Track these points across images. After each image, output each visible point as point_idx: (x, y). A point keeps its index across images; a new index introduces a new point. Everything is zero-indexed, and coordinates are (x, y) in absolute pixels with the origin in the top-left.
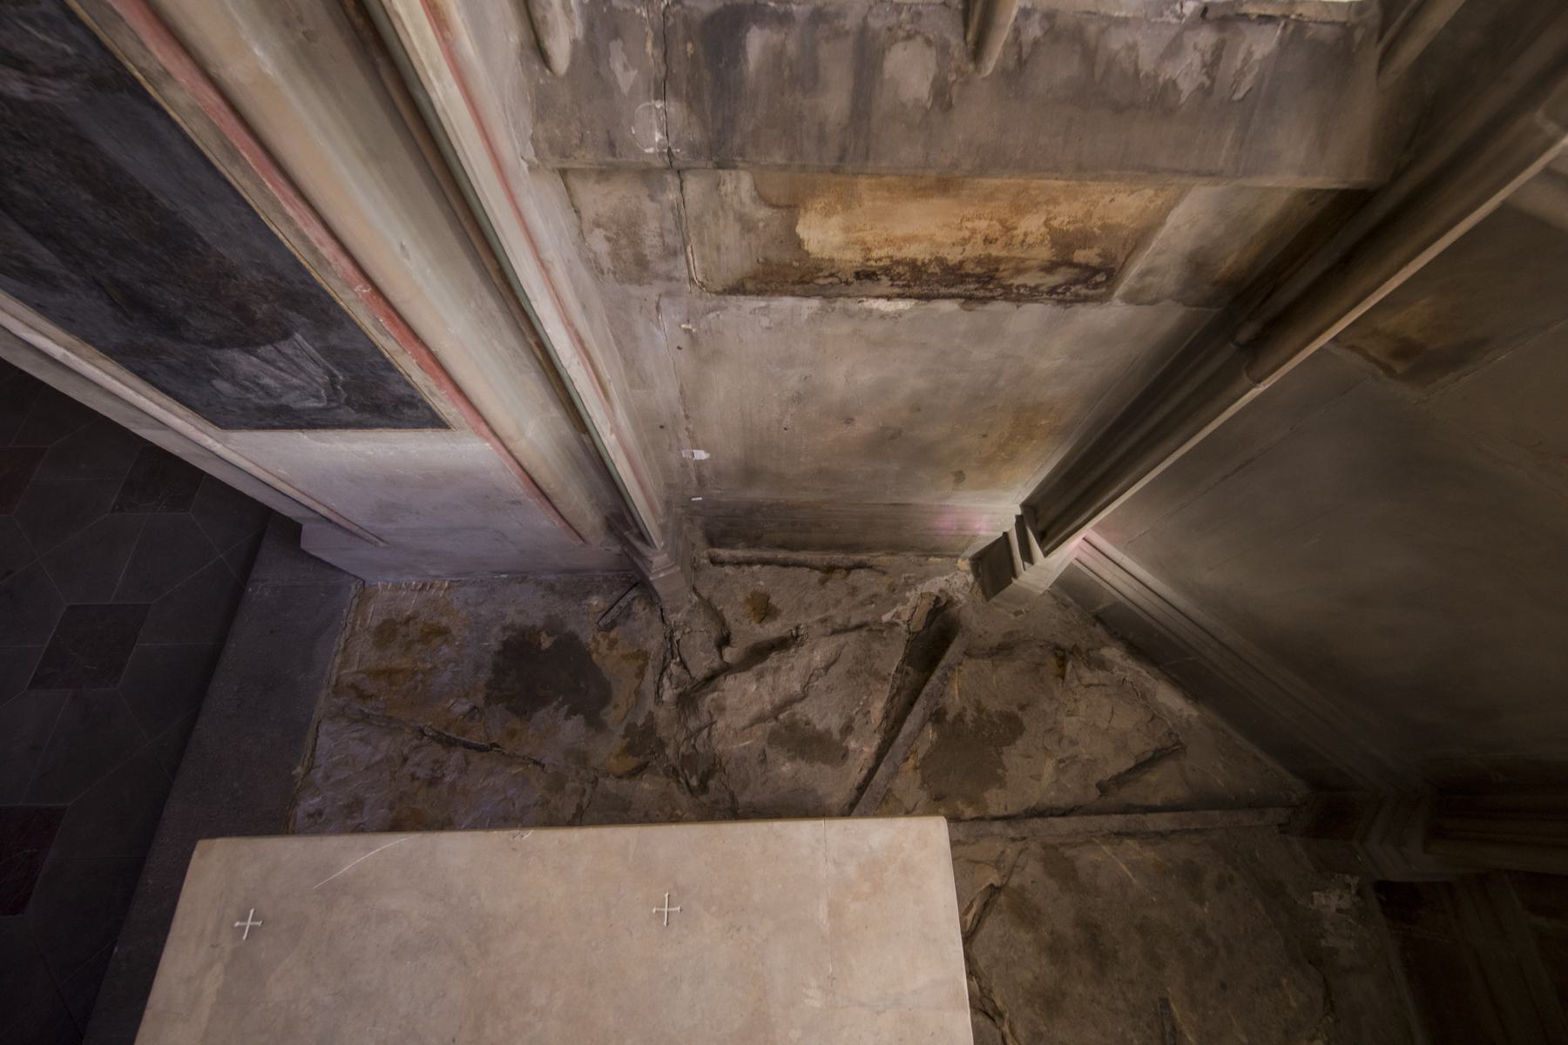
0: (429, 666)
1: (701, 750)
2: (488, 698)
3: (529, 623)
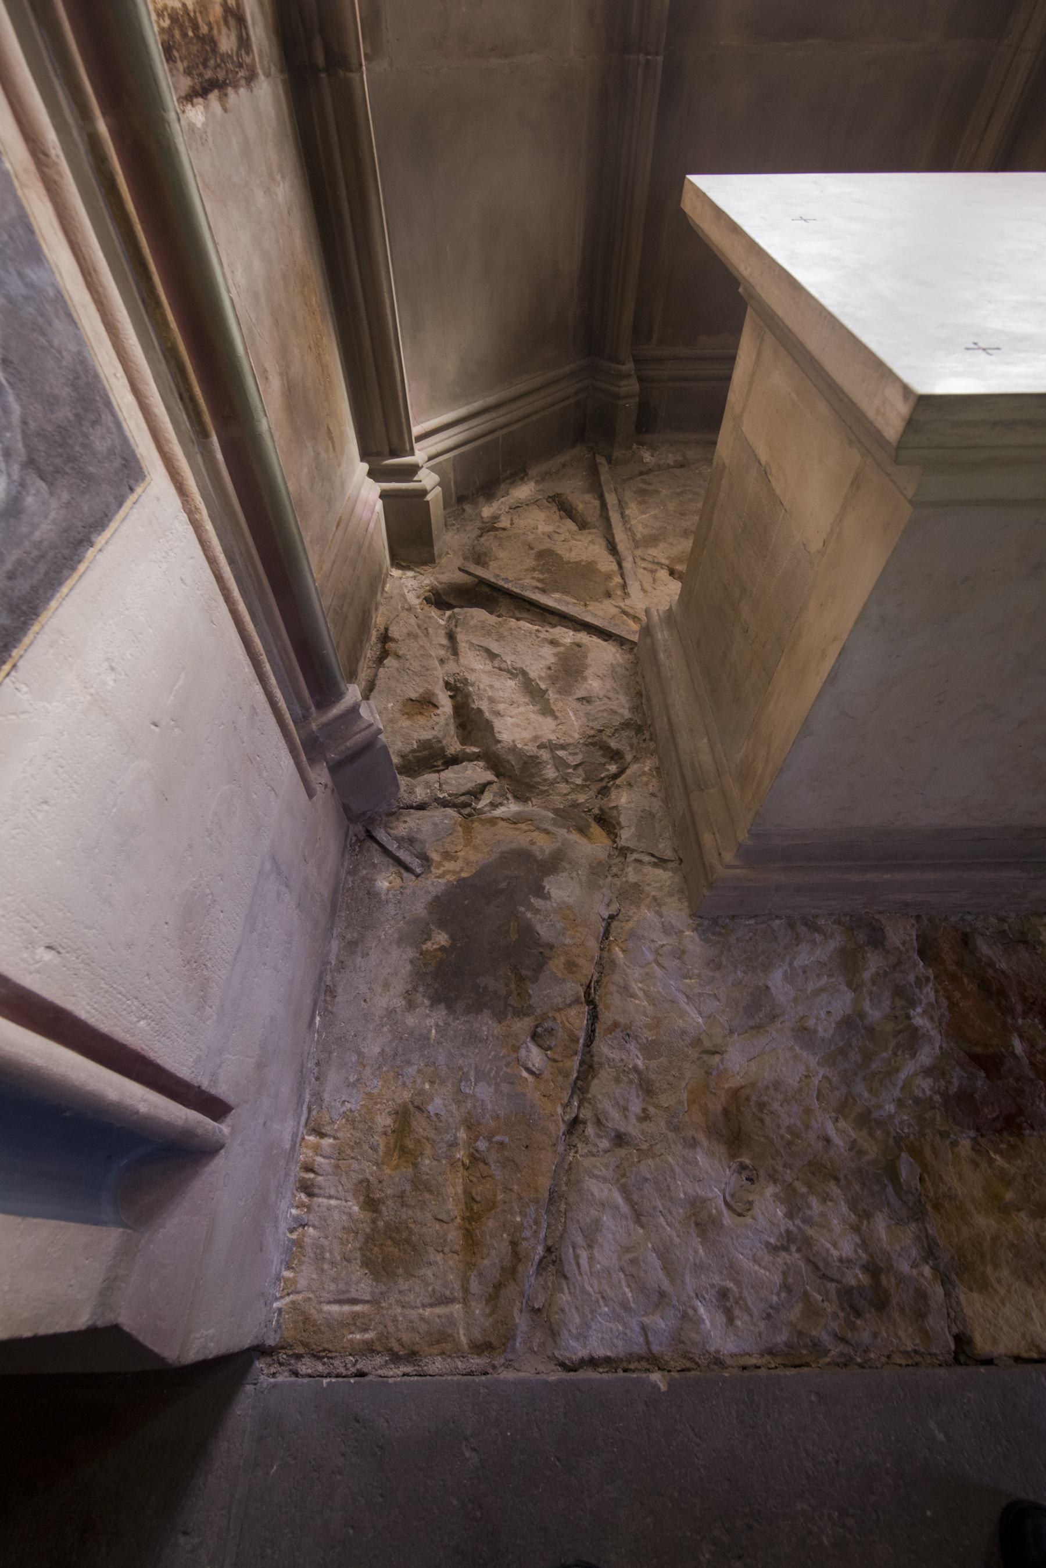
0: (462, 1135)
1: (579, 758)
2: (521, 1013)
3: (406, 969)
